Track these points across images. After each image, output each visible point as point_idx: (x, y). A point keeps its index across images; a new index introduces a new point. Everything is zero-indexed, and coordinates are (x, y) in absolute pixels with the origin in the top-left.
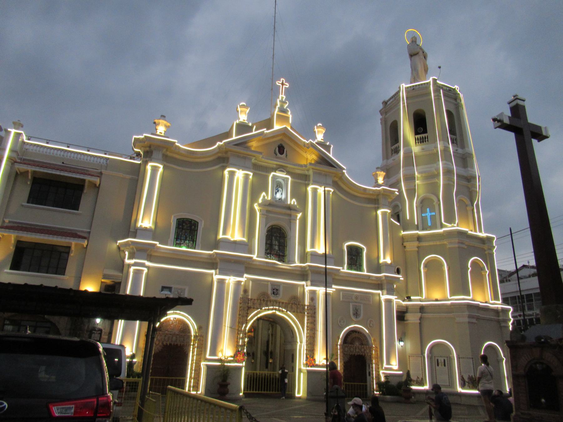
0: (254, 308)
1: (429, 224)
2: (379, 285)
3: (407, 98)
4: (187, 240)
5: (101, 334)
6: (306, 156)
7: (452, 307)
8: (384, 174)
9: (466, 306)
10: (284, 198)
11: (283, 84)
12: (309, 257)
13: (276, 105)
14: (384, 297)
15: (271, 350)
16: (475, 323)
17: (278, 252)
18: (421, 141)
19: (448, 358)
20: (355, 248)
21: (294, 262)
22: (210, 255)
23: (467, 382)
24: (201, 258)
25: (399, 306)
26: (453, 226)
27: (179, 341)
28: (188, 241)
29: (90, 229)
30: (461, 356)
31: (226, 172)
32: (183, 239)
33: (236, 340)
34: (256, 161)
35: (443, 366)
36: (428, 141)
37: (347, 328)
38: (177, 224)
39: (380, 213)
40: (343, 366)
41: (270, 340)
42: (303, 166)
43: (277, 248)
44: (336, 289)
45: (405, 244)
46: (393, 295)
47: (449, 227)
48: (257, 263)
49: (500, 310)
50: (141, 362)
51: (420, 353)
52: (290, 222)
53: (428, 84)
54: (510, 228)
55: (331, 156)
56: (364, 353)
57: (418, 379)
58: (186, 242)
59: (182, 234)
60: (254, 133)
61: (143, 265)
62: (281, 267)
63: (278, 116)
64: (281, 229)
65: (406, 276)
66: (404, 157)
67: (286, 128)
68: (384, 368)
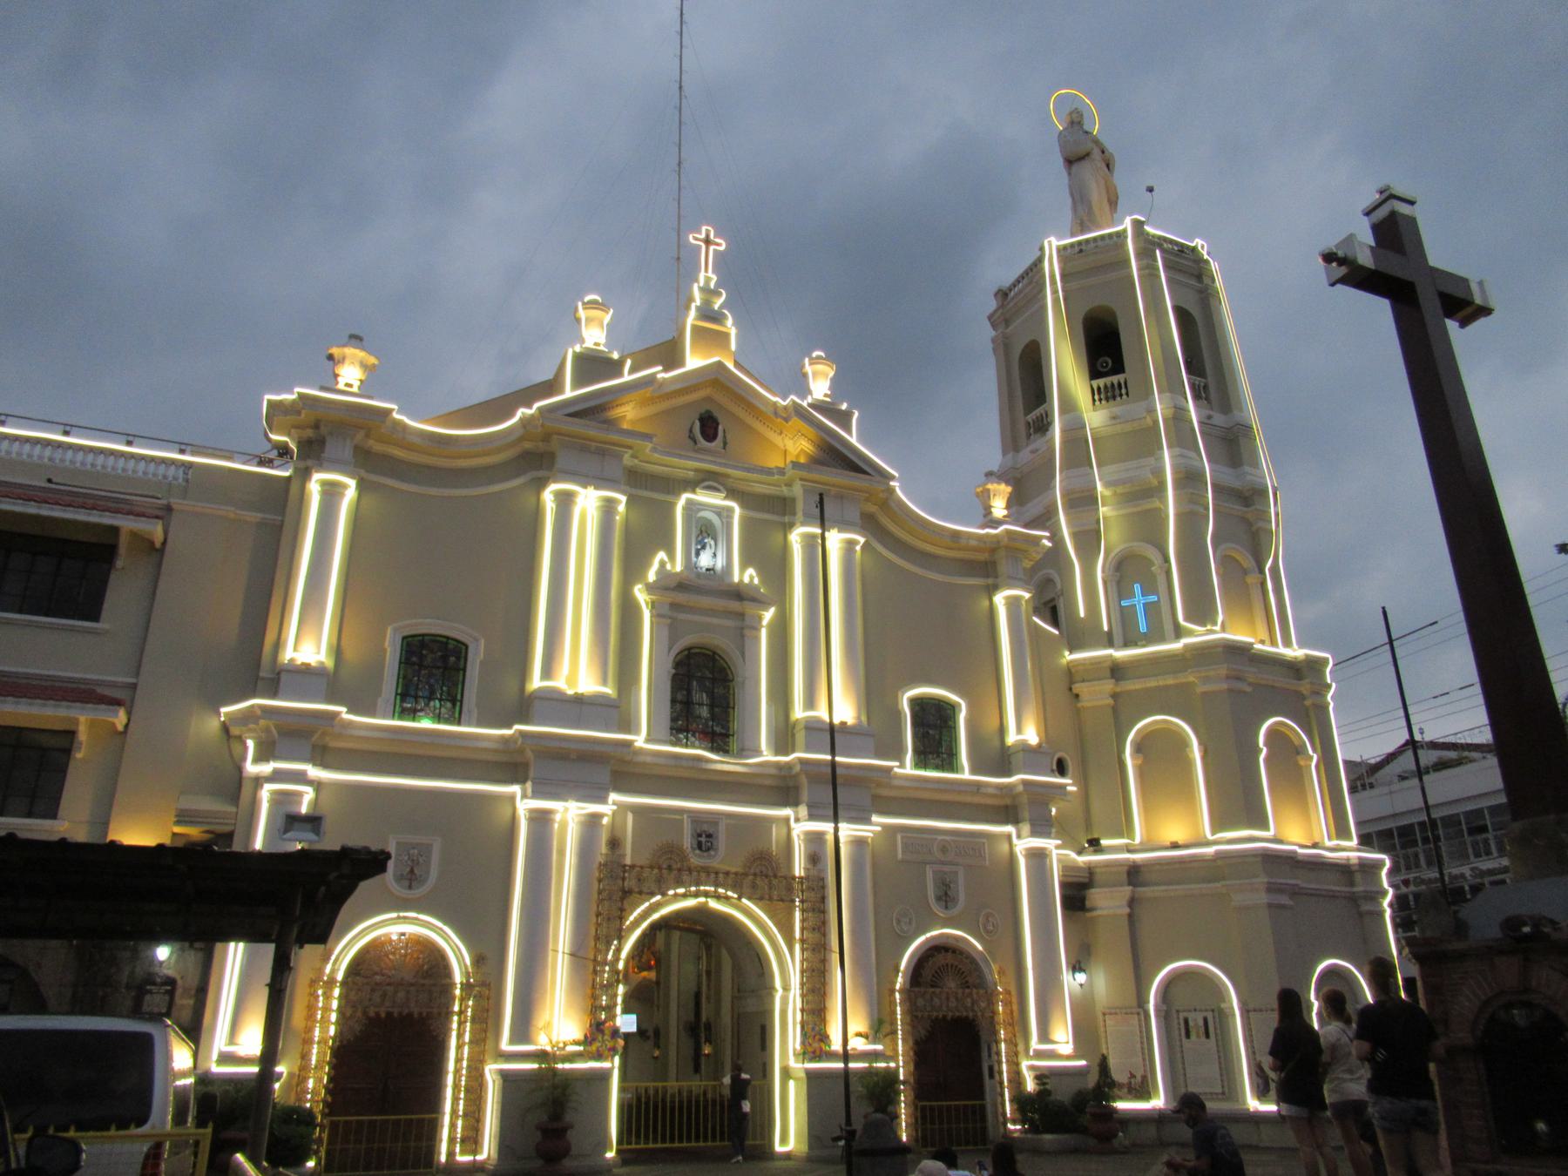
0: (640, 893)
1: (1143, 628)
2: (1007, 811)
3: (1063, 276)
4: (434, 699)
5: (171, 993)
6: (781, 445)
7: (1220, 862)
8: (1009, 489)
9: (1259, 859)
10: (723, 567)
11: (708, 242)
12: (800, 737)
13: (691, 299)
14: (1023, 843)
15: (708, 1019)
16: (1283, 907)
17: (711, 723)
18: (1108, 395)
19: (1216, 1014)
20: (935, 705)
21: (758, 752)
22: (505, 740)
23: (1273, 1080)
24: (477, 749)
25: (1067, 869)
27: (417, 1001)
28: (437, 701)
29: (137, 674)
30: (1251, 1006)
31: (548, 497)
32: (423, 697)
33: (589, 991)
34: (636, 461)
35: (1203, 1038)
36: (1127, 394)
37: (922, 939)
38: (404, 652)
39: (1003, 602)
40: (912, 1053)
41: (704, 988)
42: (775, 471)
43: (704, 712)
44: (885, 827)
45: (1077, 688)
46: (1047, 835)
47: (1199, 635)
48: (648, 759)
49: (1354, 865)
50: (297, 1073)
51: (1134, 1003)
52: (742, 636)
53: (1121, 235)
54: (1383, 608)
55: (853, 440)
56: (973, 1010)
57: (1133, 1080)
58: (432, 704)
59: (419, 680)
60: (627, 377)
61: (300, 778)
62: (719, 767)
63: (696, 330)
64: (717, 657)
65: (1084, 781)
66: (1064, 442)
67: (720, 365)
68: (1031, 1053)
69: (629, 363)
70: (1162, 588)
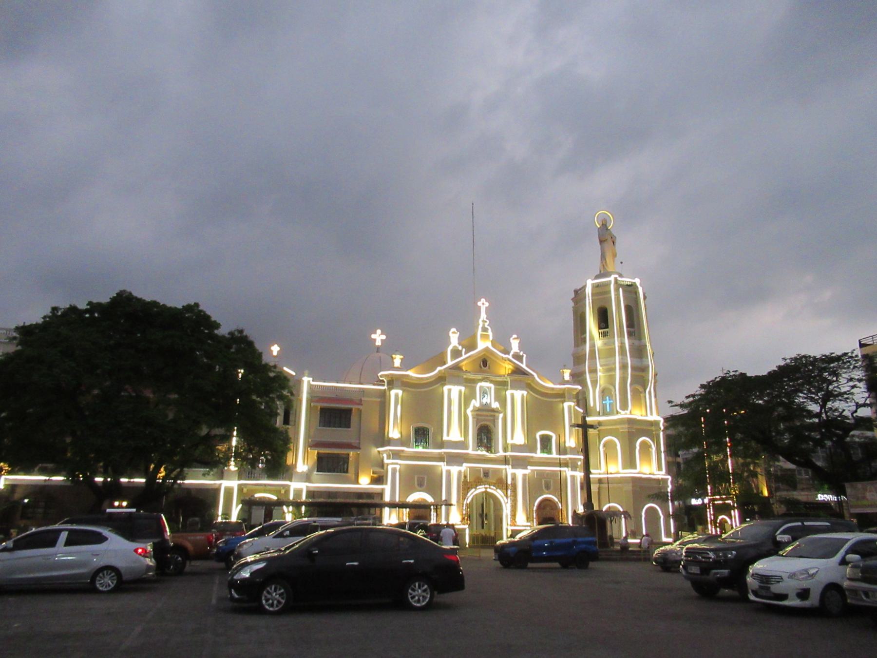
1: (608, 410)
18: (605, 335)
26: (626, 414)
43: (485, 441)
44: (532, 470)
47: (624, 415)
53: (610, 282)
60: (464, 357)
61: (397, 464)
63: (482, 336)
69: (464, 350)
70: (614, 398)
